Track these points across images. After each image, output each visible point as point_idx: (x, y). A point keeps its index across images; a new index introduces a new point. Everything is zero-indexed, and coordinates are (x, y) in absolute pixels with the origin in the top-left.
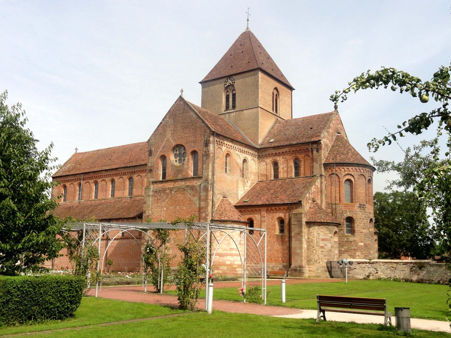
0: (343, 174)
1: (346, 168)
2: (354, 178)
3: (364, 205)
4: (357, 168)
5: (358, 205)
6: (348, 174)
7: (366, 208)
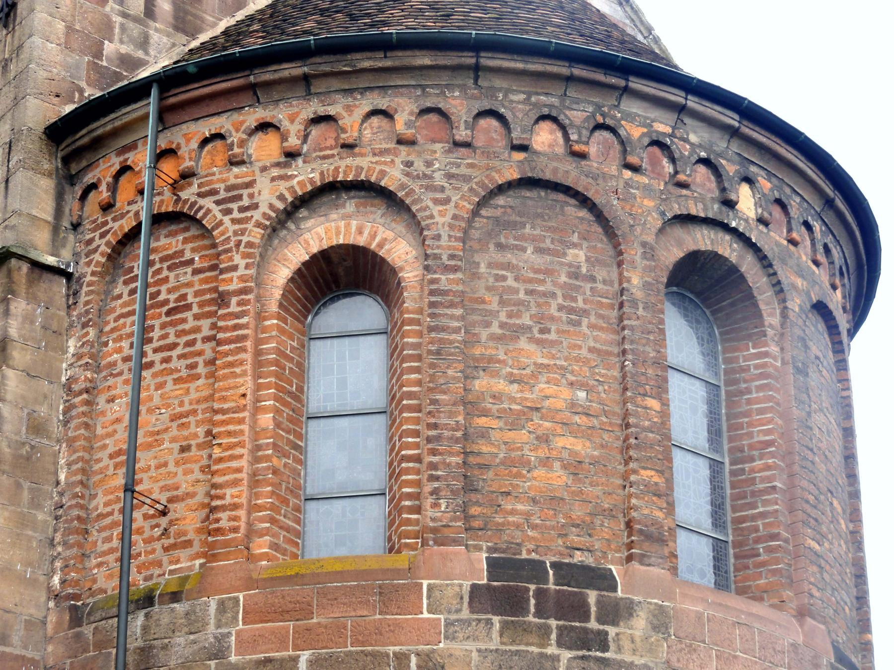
0: (269, 195)
1: (292, 114)
2: (417, 227)
3: (603, 580)
4: (459, 104)
5: (471, 566)
6: (330, 190)
7: (615, 612)
